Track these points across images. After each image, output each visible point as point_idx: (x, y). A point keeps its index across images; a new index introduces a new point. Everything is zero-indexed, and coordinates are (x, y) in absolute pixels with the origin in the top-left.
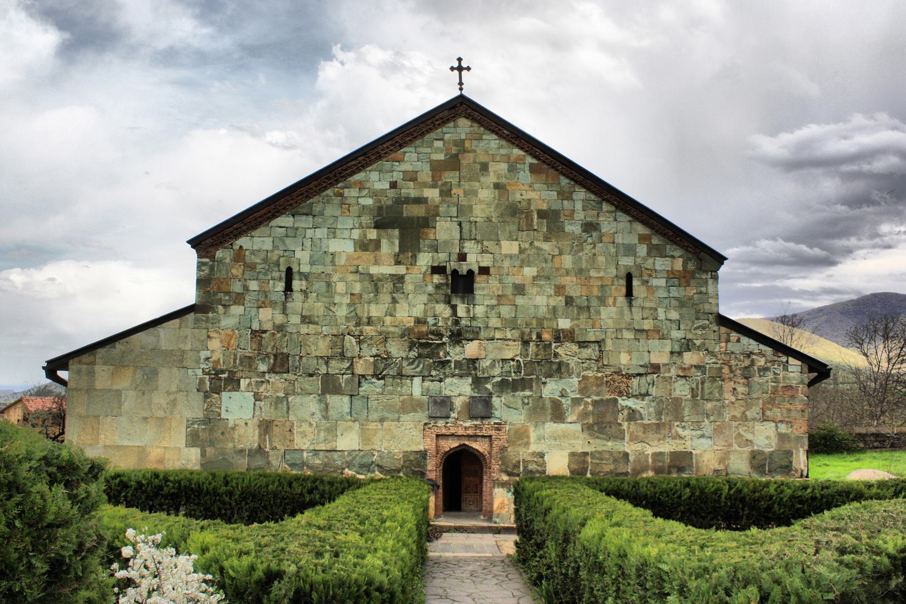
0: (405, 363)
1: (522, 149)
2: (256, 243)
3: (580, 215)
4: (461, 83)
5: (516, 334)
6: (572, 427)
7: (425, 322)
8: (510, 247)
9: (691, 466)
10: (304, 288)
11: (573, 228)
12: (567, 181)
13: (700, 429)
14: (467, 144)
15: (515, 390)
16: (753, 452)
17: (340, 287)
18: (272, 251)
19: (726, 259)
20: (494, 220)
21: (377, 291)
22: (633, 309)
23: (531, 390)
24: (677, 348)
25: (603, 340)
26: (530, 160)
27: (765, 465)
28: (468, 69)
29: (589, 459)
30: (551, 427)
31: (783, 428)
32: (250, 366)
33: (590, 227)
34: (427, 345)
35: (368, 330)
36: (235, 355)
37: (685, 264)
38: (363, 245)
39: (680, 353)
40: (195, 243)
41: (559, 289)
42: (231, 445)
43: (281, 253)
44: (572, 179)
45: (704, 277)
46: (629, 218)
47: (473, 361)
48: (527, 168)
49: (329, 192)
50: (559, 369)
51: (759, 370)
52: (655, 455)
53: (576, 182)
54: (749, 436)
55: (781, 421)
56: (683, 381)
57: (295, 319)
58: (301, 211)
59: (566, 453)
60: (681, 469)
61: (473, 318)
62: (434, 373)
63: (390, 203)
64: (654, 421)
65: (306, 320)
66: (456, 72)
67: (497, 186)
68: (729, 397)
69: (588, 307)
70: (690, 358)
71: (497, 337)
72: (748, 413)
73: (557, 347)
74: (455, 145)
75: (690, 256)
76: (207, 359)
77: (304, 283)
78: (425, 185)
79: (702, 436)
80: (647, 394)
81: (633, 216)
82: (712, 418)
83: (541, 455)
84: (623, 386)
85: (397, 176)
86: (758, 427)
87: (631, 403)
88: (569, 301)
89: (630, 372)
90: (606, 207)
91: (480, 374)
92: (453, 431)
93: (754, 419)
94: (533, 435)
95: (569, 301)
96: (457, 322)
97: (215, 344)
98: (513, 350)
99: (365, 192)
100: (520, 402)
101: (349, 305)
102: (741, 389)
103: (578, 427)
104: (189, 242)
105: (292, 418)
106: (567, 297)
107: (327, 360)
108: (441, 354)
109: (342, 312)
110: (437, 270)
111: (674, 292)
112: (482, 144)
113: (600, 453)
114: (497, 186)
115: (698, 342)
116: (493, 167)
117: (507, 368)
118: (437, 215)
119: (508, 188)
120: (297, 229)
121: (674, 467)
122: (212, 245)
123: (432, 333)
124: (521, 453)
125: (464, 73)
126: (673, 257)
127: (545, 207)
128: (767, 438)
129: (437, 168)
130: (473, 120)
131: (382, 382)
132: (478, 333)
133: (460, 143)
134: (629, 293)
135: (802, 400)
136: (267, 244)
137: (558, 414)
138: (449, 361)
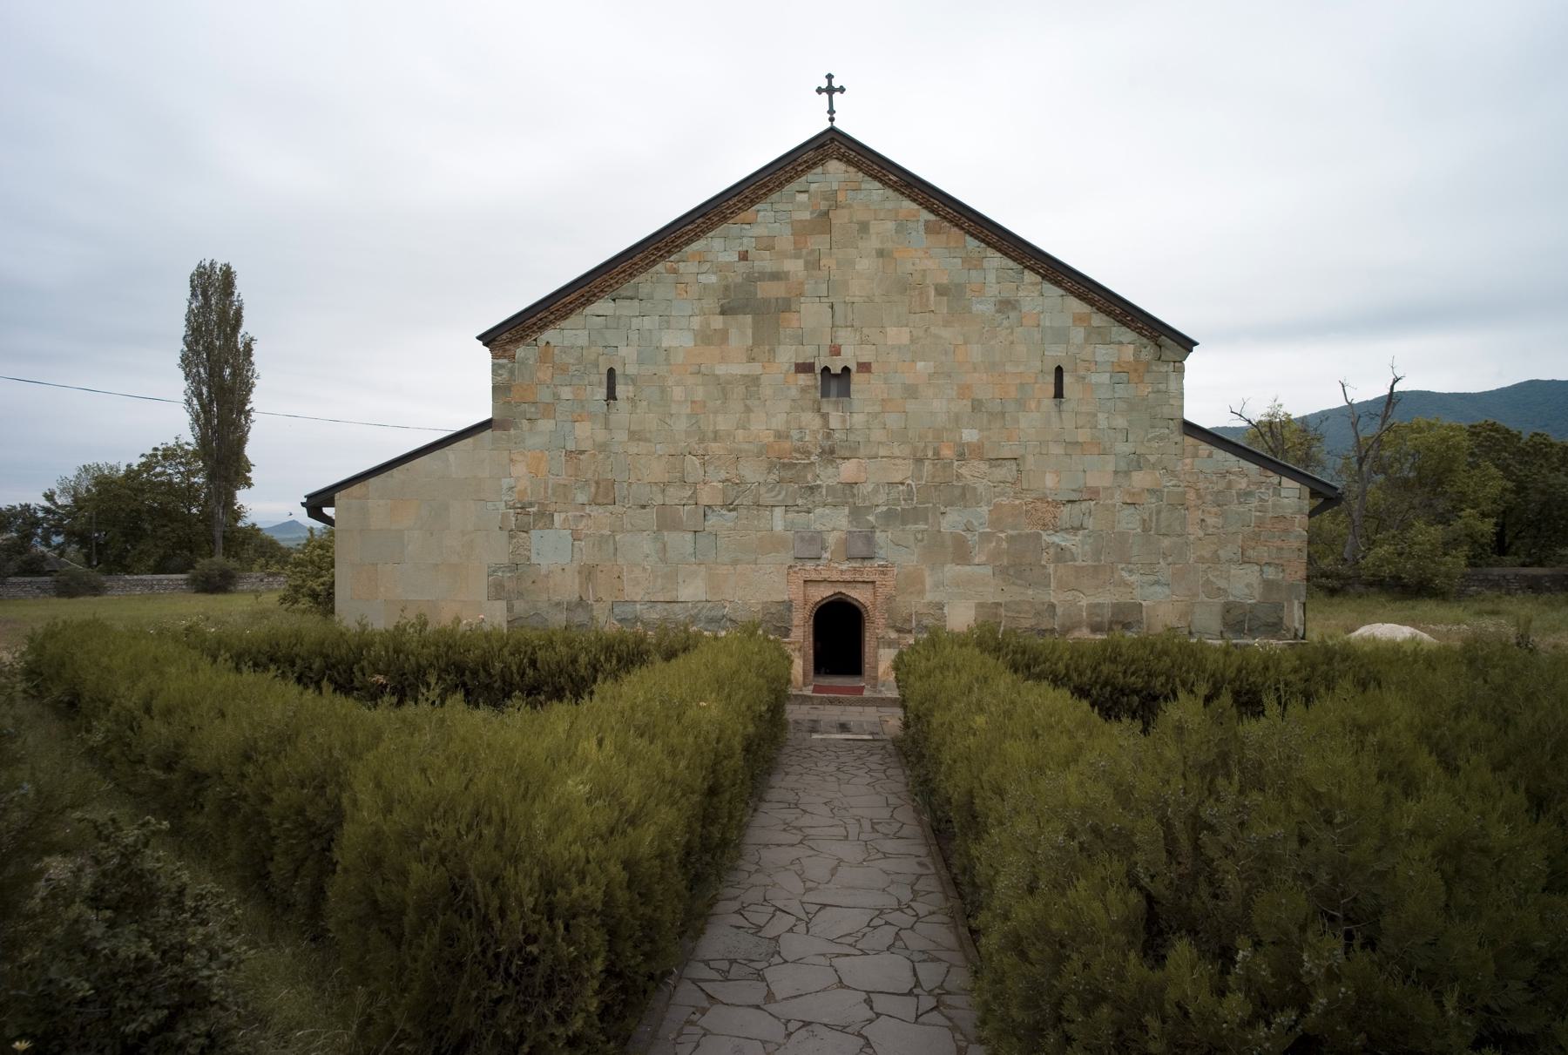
0: (763, 490)
1: (914, 200)
2: (564, 336)
3: (993, 289)
4: (831, 111)
5: (907, 450)
6: (979, 570)
7: (788, 437)
8: (897, 335)
9: (1140, 622)
10: (631, 395)
11: (983, 308)
12: (977, 243)
13: (1153, 574)
14: (841, 197)
15: (904, 523)
16: (1226, 603)
17: (678, 393)
18: (589, 347)
19: (1196, 344)
20: (877, 299)
21: (725, 398)
22: (1064, 415)
23: (926, 521)
24: (1123, 466)
25: (1023, 456)
26: (926, 215)
27: (1243, 621)
28: (842, 90)
29: (1002, 611)
30: (952, 570)
31: (1271, 573)
32: (566, 497)
33: (1007, 305)
34: (791, 469)
35: (714, 447)
36: (546, 483)
37: (1137, 353)
38: (706, 337)
39: (1127, 473)
40: (488, 338)
41: (964, 390)
42: (545, 597)
43: (601, 350)
44: (983, 241)
45: (1164, 368)
47: (852, 485)
48: (921, 223)
49: (659, 267)
50: (963, 495)
51: (1239, 495)
52: (1091, 606)
53: (988, 244)
54: (1222, 584)
55: (1268, 564)
56: (1132, 510)
57: (621, 436)
58: (625, 294)
59: (972, 603)
60: (1127, 626)
61: (849, 430)
62: (800, 502)
63: (739, 280)
64: (1090, 563)
65: (635, 436)
66: (825, 96)
67: (881, 253)
68: (1195, 532)
69: (1003, 414)
70: (1140, 480)
71: (882, 453)
72: (1221, 553)
73: (960, 467)
74: (826, 199)
75: (1145, 341)
76: (511, 488)
77: (631, 388)
78: (784, 255)
79: (1157, 583)
80: (1082, 527)
81: (1066, 289)
83: (940, 606)
84: (1049, 517)
85: (748, 244)
86: (1235, 570)
87: (1056, 539)
88: (977, 405)
89: (1058, 498)
90: (1029, 276)
91: (859, 503)
92: (825, 575)
93: (1230, 561)
94: (929, 582)
95: (977, 405)
96: (828, 436)
97: (519, 470)
98: (902, 471)
99: (706, 267)
100: (912, 538)
101: (689, 416)
102: (1211, 521)
103: (988, 570)
104: (479, 338)
105: (620, 561)
106: (973, 400)
107: (664, 487)
108: (809, 477)
109: (681, 425)
110: (804, 368)
111: (1121, 391)
112: (861, 195)
113: (1017, 603)
114: (881, 253)
115: (1152, 459)
116: (875, 227)
117: (894, 495)
118: (801, 295)
119: (896, 255)
120: (619, 318)
121: (1117, 622)
122: (511, 342)
123: (797, 450)
124: (911, 604)
125: (836, 96)
126: (1121, 343)
127: (945, 280)
128: (1247, 586)
129: (801, 231)
130: (849, 162)
131: (734, 514)
132: (856, 449)
133: (831, 197)
134: (1059, 393)
135: (1300, 535)
136: (582, 338)
137: (962, 553)
138: (819, 486)
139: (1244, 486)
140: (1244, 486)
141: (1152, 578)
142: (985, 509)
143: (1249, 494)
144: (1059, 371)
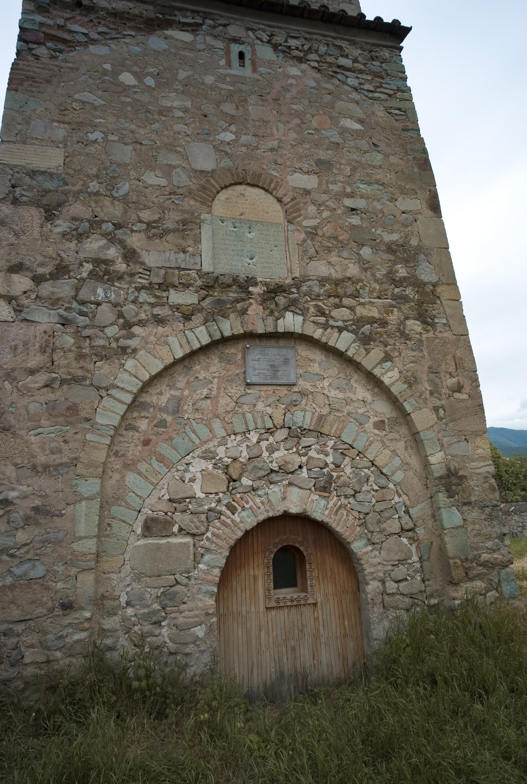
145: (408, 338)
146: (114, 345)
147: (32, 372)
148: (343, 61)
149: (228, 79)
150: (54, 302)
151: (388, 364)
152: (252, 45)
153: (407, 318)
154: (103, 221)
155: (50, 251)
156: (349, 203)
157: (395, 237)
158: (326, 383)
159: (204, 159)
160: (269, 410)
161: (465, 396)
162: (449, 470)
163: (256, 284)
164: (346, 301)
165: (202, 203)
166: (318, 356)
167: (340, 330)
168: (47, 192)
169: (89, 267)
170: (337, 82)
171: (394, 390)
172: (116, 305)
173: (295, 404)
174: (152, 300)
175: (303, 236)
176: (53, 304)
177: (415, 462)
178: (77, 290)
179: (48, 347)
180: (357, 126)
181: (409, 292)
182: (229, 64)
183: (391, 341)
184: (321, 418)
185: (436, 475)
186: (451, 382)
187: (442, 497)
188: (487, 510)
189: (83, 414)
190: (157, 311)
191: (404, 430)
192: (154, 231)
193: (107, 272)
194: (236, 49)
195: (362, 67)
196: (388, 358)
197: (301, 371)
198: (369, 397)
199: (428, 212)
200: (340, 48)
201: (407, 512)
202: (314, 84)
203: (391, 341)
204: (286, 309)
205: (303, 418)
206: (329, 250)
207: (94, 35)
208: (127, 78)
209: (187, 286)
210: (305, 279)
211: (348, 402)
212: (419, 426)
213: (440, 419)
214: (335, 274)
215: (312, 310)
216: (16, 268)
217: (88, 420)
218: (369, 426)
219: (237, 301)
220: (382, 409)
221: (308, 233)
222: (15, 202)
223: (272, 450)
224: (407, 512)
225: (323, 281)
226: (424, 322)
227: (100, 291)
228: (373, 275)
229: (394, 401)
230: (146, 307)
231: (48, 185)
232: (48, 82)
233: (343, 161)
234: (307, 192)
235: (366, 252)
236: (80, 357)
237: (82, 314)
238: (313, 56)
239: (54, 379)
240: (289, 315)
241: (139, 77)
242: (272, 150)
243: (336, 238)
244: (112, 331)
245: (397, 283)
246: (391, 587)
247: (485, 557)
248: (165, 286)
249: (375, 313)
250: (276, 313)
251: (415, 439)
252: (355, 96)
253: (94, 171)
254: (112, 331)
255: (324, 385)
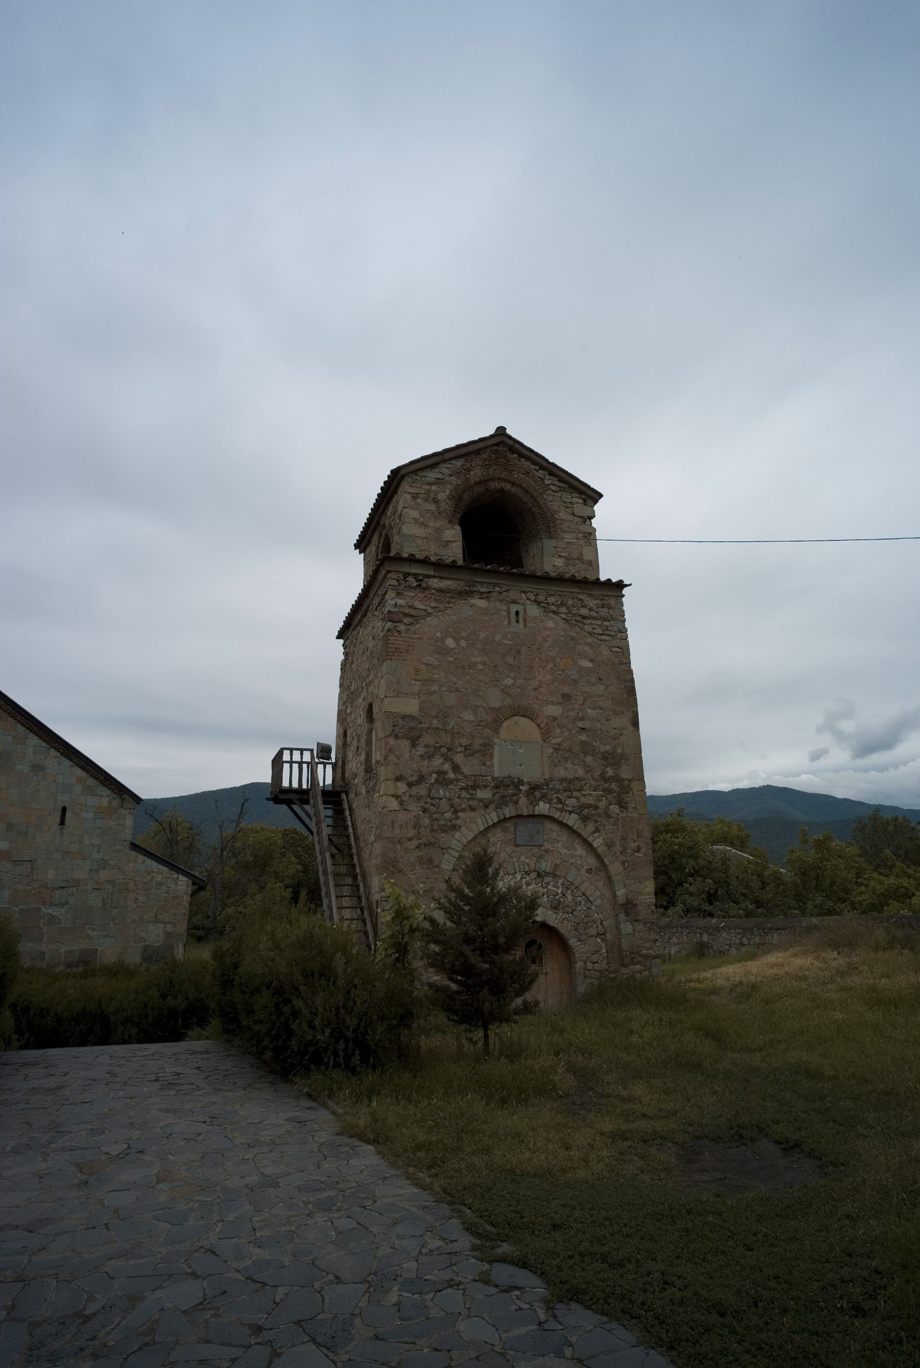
12: (24, 729)
31: (169, 928)
39: (97, 871)
44: (28, 728)
45: (124, 812)
46: (70, 763)
53: (31, 731)
55: (169, 923)
70: (104, 875)
79: (107, 936)
80: (67, 903)
81: (74, 762)
82: (116, 921)
90: (53, 752)
115: (112, 863)
134: (62, 823)
139: (159, 879)
140: (159, 879)
141: (105, 933)
142: (7, 892)
143: (161, 884)
144: (64, 809)
145: (609, 817)
146: (449, 824)
147: (410, 839)
148: (584, 612)
149: (509, 636)
150: (419, 798)
151: (597, 834)
152: (524, 605)
153: (611, 804)
154: (441, 747)
155: (415, 766)
156: (580, 724)
157: (607, 747)
158: (560, 845)
159: (495, 700)
160: (527, 861)
161: (641, 855)
162: (627, 899)
163: (523, 785)
164: (576, 794)
165: (495, 731)
166: (556, 828)
167: (570, 812)
168: (412, 728)
169: (435, 776)
170: (578, 629)
171: (599, 850)
172: (449, 799)
173: (541, 857)
174: (468, 796)
175: (551, 750)
176: (418, 800)
177: (608, 894)
178: (430, 791)
179: (417, 826)
180: (589, 665)
181: (613, 786)
182: (509, 623)
183: (600, 819)
184: (556, 865)
185: (620, 902)
186: (634, 845)
187: (622, 916)
188: (648, 925)
189: (435, 863)
190: (471, 803)
191: (603, 874)
192: (468, 752)
193: (444, 779)
194: (514, 608)
195: (595, 614)
196: (597, 830)
197: (546, 837)
198: (584, 854)
199: (631, 728)
200: (582, 600)
201: (601, 923)
202: (563, 633)
203: (600, 819)
204: (540, 800)
205: (546, 866)
206: (566, 759)
207: (430, 610)
208: (450, 643)
209: (486, 786)
210: (551, 779)
211: (573, 856)
212: (612, 873)
213: (625, 869)
214: (570, 775)
215: (555, 800)
216: (399, 778)
217: (438, 866)
218: (583, 872)
219: (514, 795)
220: (592, 861)
221: (555, 749)
222: (396, 737)
223: (528, 884)
224: (601, 923)
225: (562, 780)
226: (621, 806)
227: (441, 791)
228: (592, 775)
229: (599, 857)
230: (465, 800)
231: (412, 724)
232: (407, 651)
233: (579, 694)
234: (555, 718)
235: (589, 759)
236: (433, 831)
237: (433, 805)
238: (563, 609)
239: (421, 844)
240: (541, 803)
241: (456, 641)
242: (535, 689)
243: (570, 751)
244: (448, 815)
245: (607, 780)
246: (590, 966)
247: (644, 952)
248: (475, 787)
249: (591, 801)
250: (534, 803)
251: (609, 880)
252: (589, 640)
253: (435, 713)
254: (448, 815)
255: (558, 845)
